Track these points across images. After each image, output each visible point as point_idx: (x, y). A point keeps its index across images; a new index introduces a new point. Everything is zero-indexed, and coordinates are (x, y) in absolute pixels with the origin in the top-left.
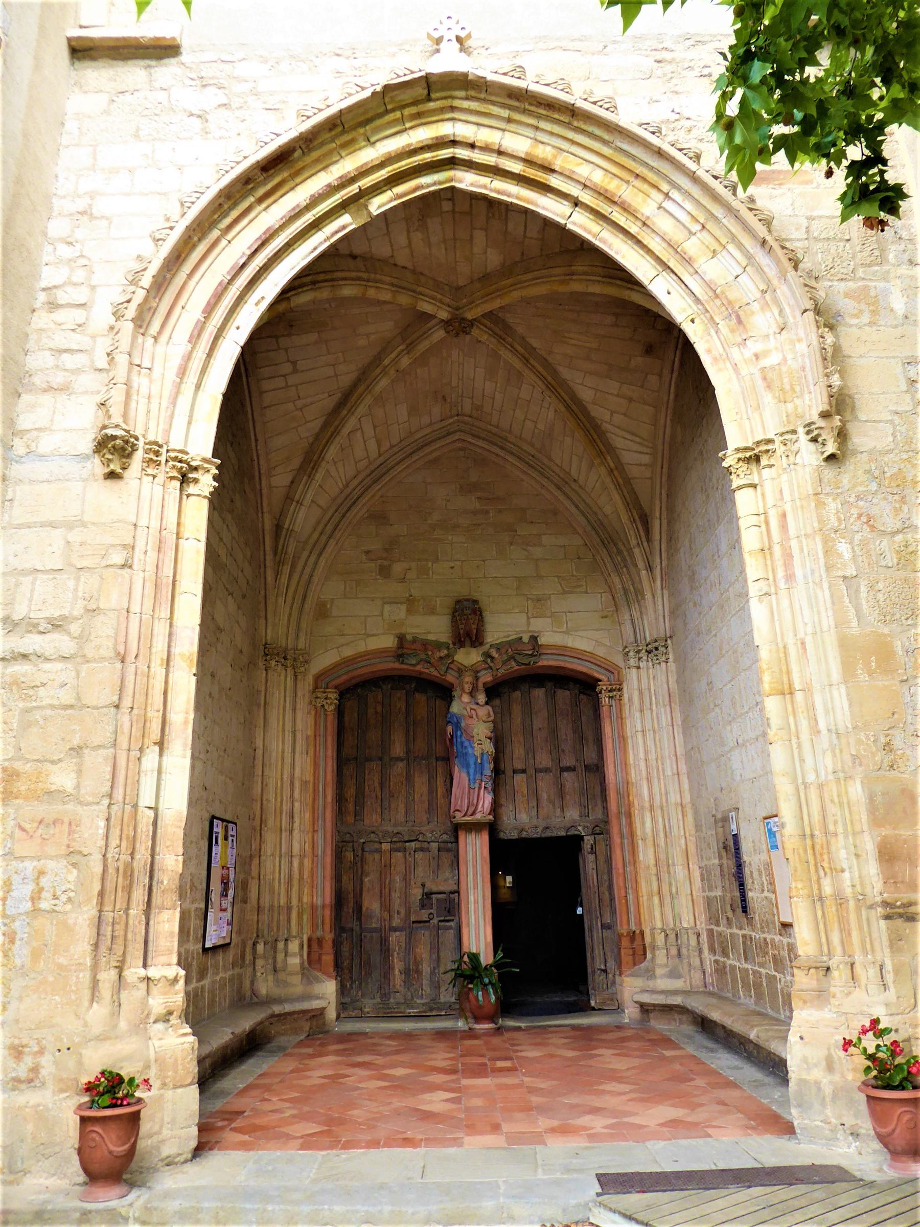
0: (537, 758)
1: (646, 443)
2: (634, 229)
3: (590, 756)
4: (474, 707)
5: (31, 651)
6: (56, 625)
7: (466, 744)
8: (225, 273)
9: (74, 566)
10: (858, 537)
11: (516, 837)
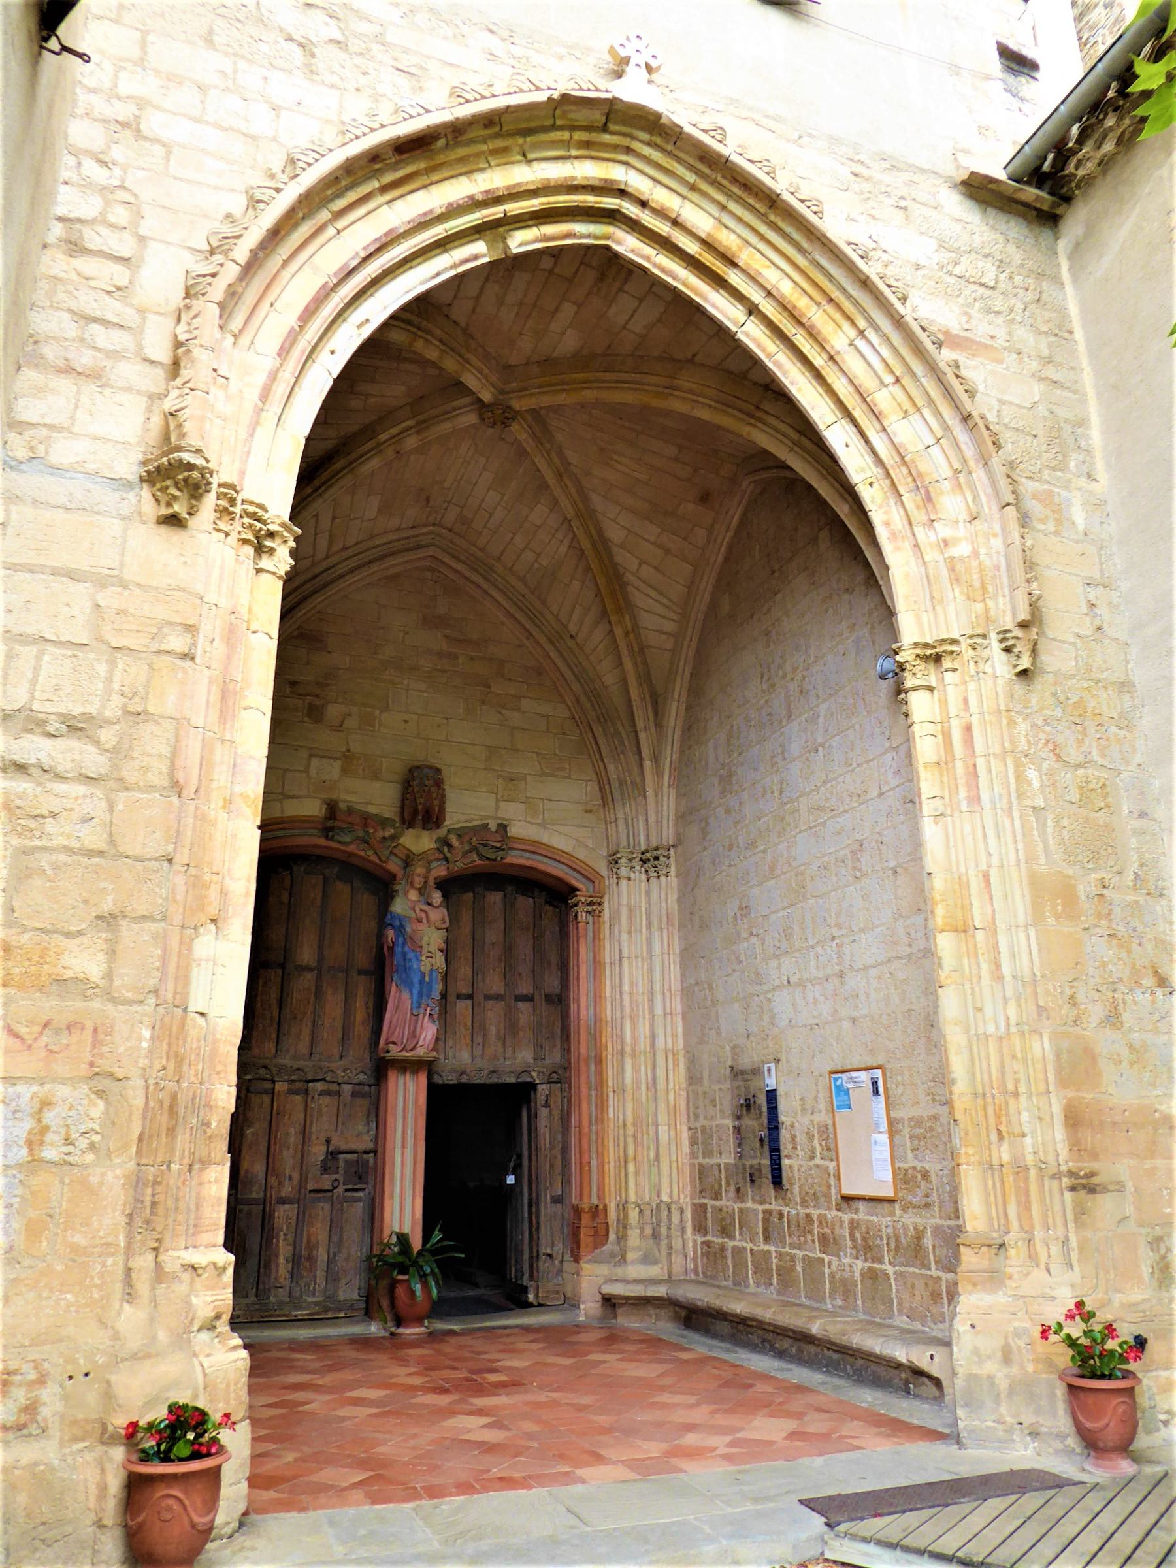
1: (674, 608)
2: (819, 361)
3: (552, 983)
4: (426, 907)
5: (33, 761)
6: (75, 727)
7: (411, 955)
8: (331, 273)
9: (108, 644)
10: (1045, 765)
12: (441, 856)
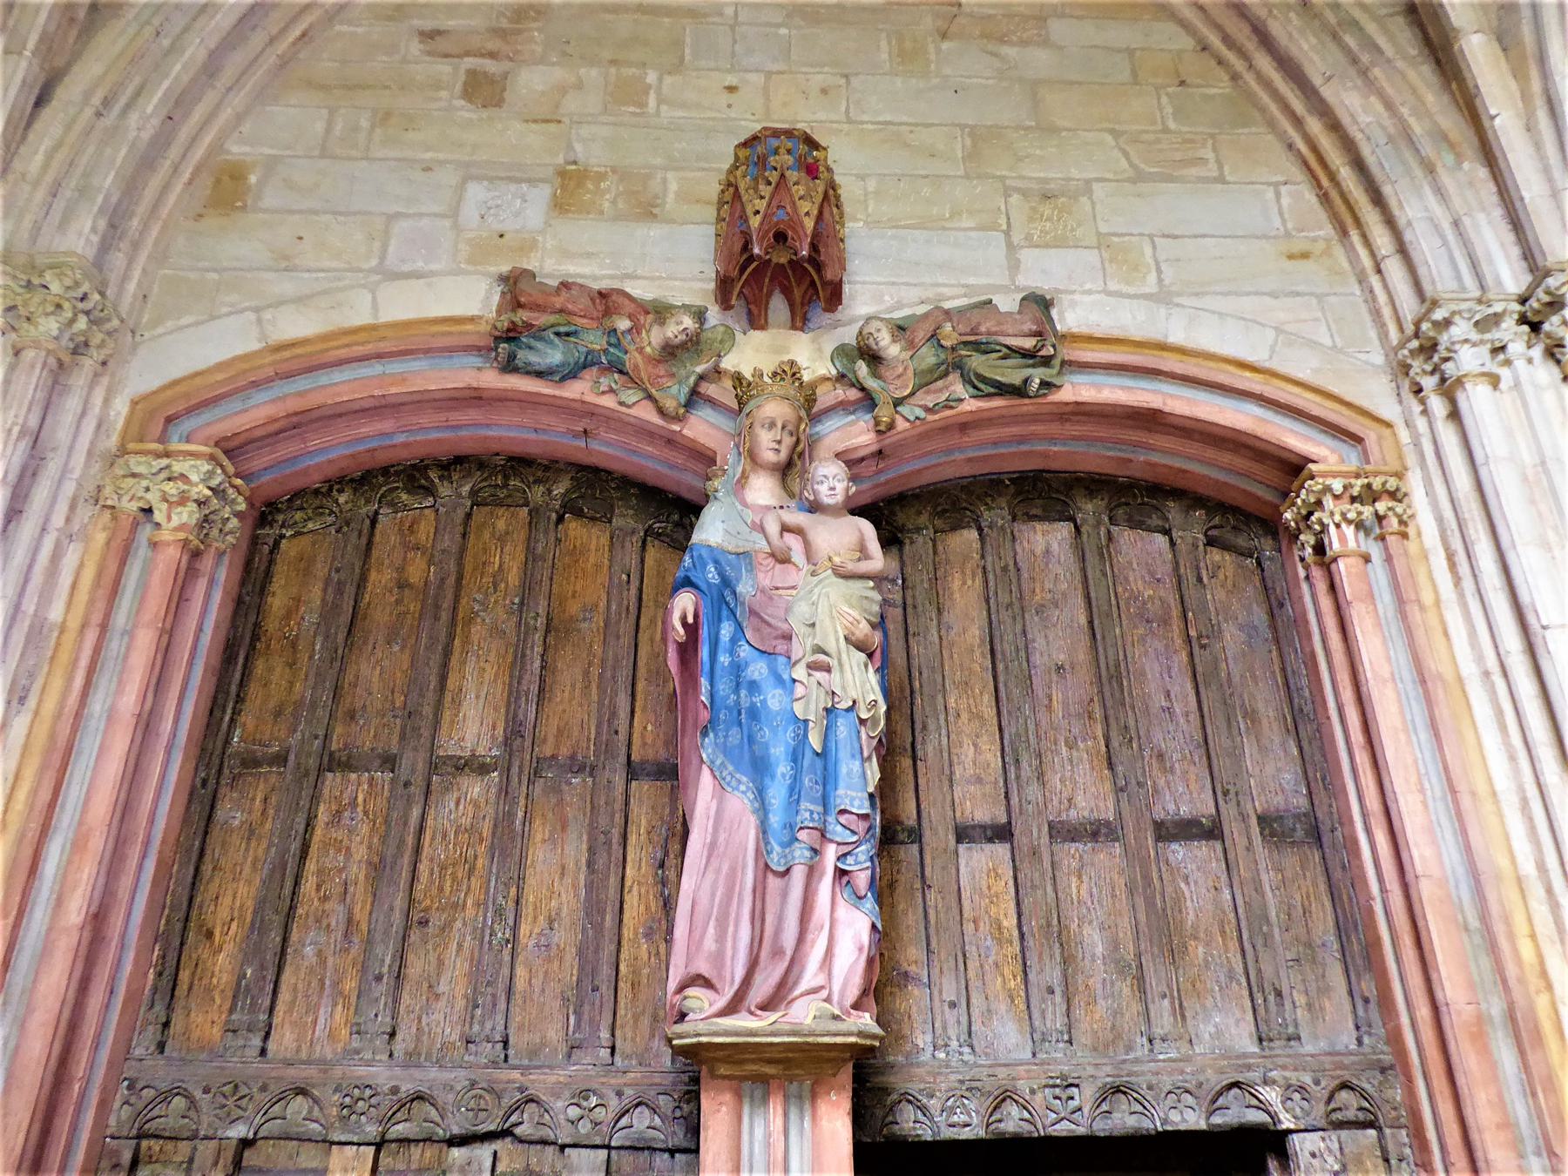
0: (1055, 780)
7: (758, 669)
11: (975, 1131)
12: (853, 394)
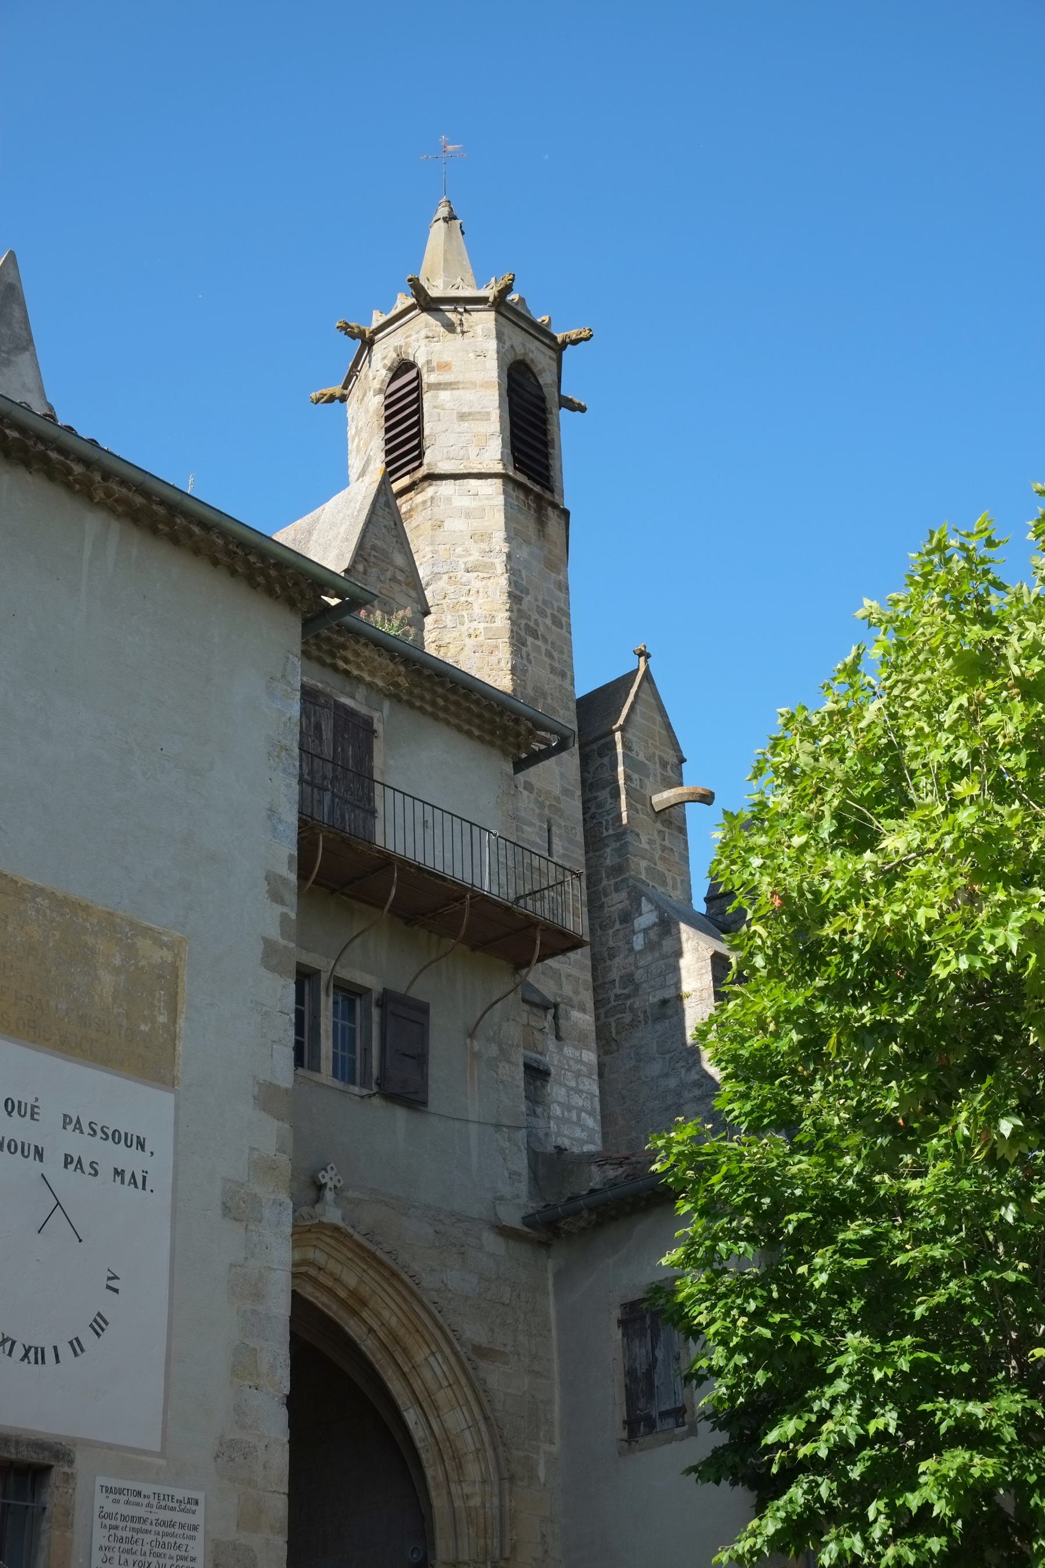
2: (406, 1369)
